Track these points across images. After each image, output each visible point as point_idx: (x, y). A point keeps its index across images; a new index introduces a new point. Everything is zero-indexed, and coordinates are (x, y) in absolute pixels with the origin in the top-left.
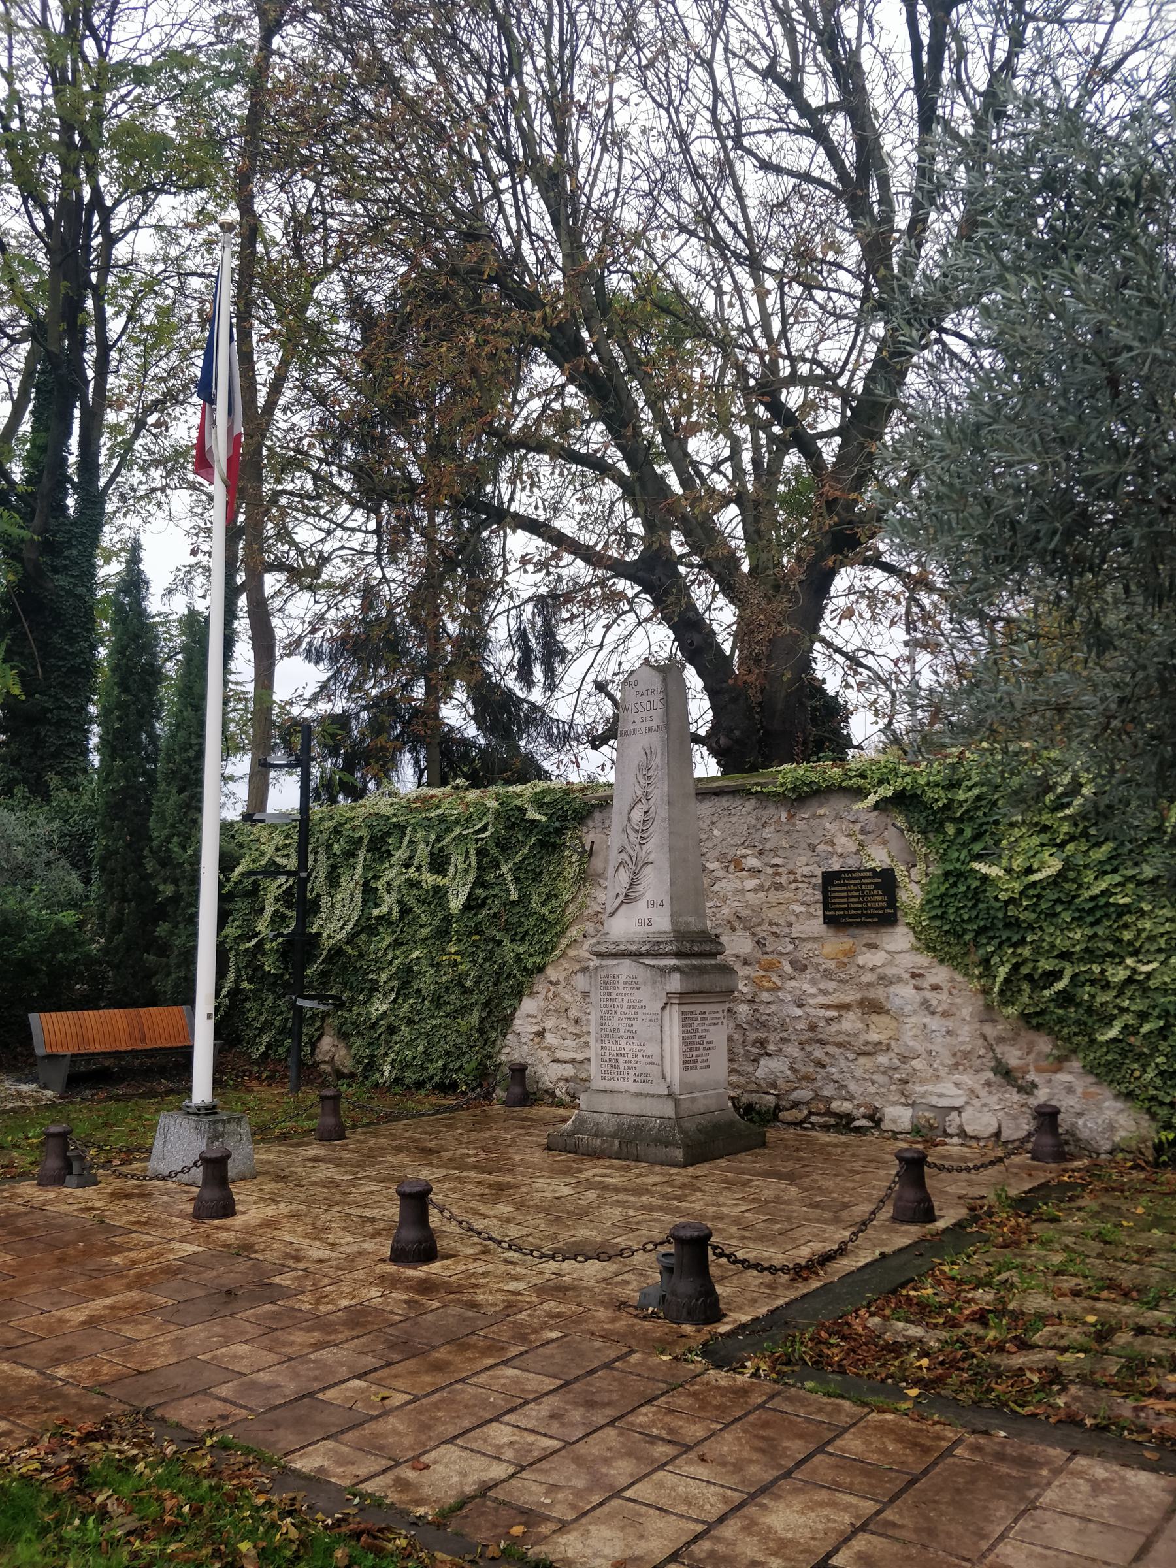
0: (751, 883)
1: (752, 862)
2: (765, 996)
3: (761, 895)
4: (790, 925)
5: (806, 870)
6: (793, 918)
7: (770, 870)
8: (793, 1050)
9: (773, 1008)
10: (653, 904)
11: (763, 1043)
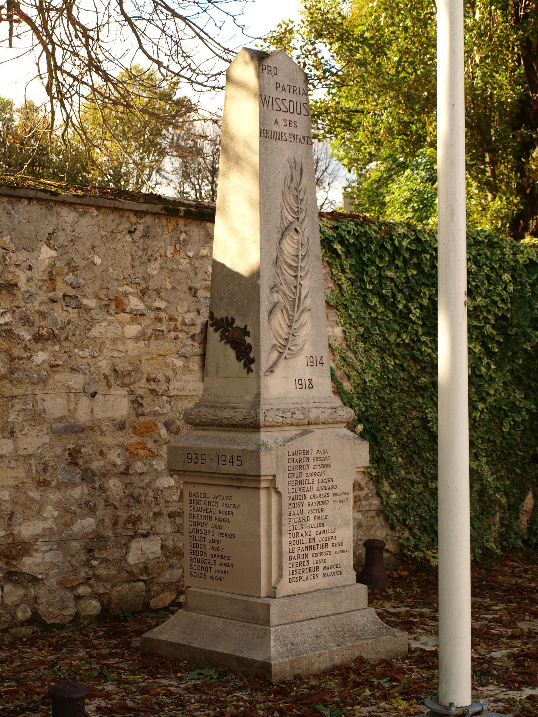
0: (133, 330)
1: (135, 303)
2: (139, 466)
3: (141, 344)
4: (168, 381)
5: (188, 317)
6: (170, 373)
7: (152, 315)
8: (165, 526)
9: (147, 479)
10: (312, 362)
11: (134, 521)
